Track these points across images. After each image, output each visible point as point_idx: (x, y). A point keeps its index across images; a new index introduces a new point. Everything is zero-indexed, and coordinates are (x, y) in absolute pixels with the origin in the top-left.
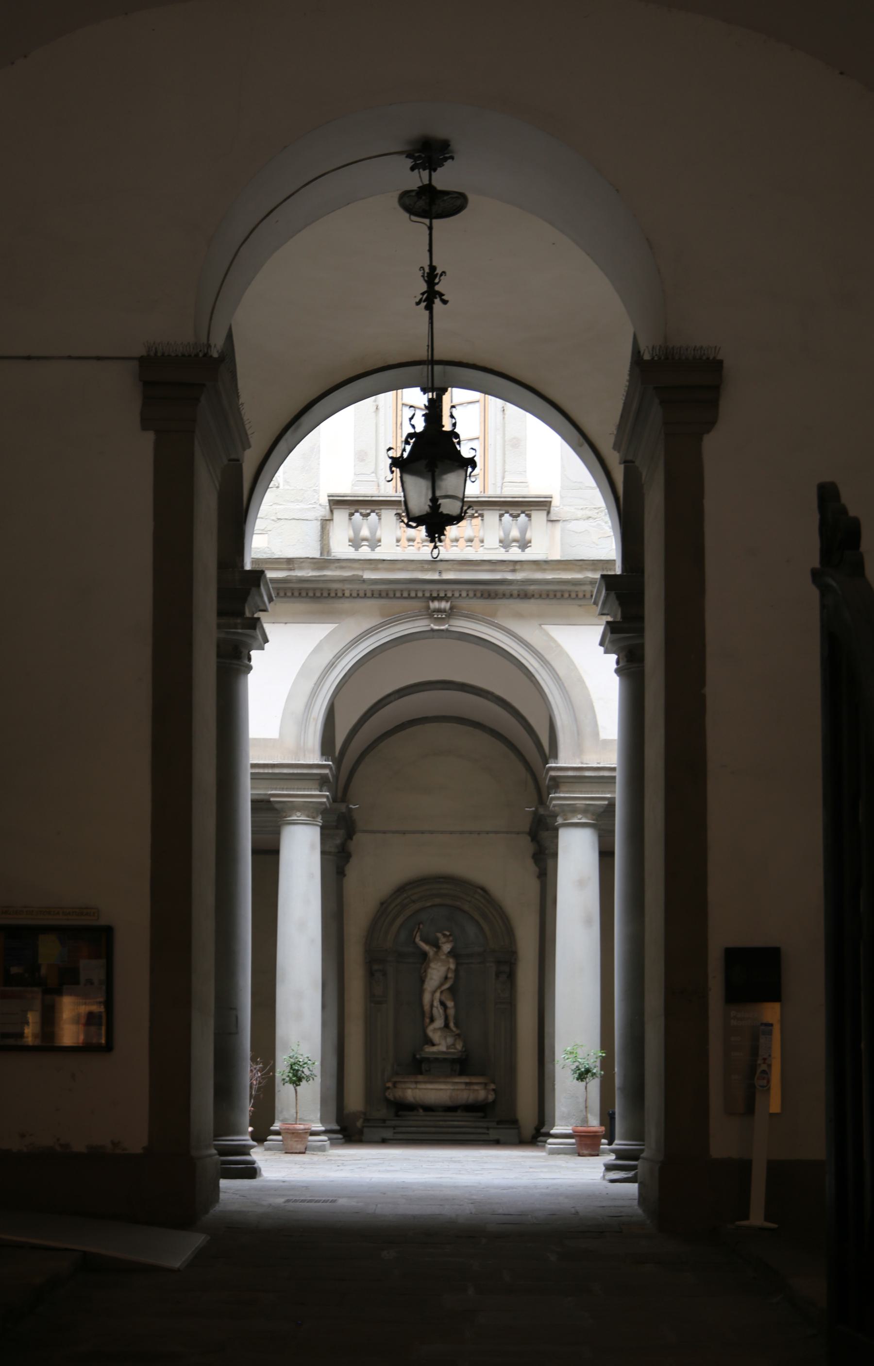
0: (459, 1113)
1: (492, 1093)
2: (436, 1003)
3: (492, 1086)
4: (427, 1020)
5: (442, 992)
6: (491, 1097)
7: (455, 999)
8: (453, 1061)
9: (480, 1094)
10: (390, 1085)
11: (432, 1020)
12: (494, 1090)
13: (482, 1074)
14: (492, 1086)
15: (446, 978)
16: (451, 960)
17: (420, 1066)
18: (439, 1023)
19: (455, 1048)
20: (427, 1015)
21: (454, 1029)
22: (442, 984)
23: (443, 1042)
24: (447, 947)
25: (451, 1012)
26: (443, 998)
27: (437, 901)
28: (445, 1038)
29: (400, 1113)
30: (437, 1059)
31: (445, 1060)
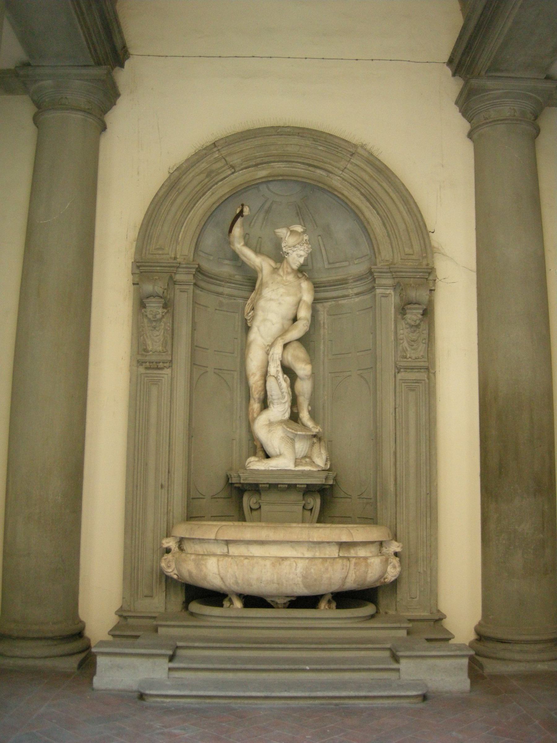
0: (325, 610)
1: (395, 561)
2: (274, 368)
3: (395, 547)
4: (256, 406)
5: (285, 346)
6: (392, 573)
7: (312, 358)
8: (309, 490)
9: (371, 568)
10: (170, 543)
11: (265, 404)
12: (396, 554)
13: (370, 520)
14: (395, 547)
15: (295, 319)
16: (305, 285)
17: (242, 497)
18: (279, 410)
19: (313, 463)
20: (256, 394)
21: (310, 424)
22: (284, 332)
23: (285, 449)
24: (297, 256)
25: (304, 387)
26: (289, 358)
27: (280, 168)
28: (292, 441)
29: (195, 607)
30: (273, 487)
31: (291, 487)
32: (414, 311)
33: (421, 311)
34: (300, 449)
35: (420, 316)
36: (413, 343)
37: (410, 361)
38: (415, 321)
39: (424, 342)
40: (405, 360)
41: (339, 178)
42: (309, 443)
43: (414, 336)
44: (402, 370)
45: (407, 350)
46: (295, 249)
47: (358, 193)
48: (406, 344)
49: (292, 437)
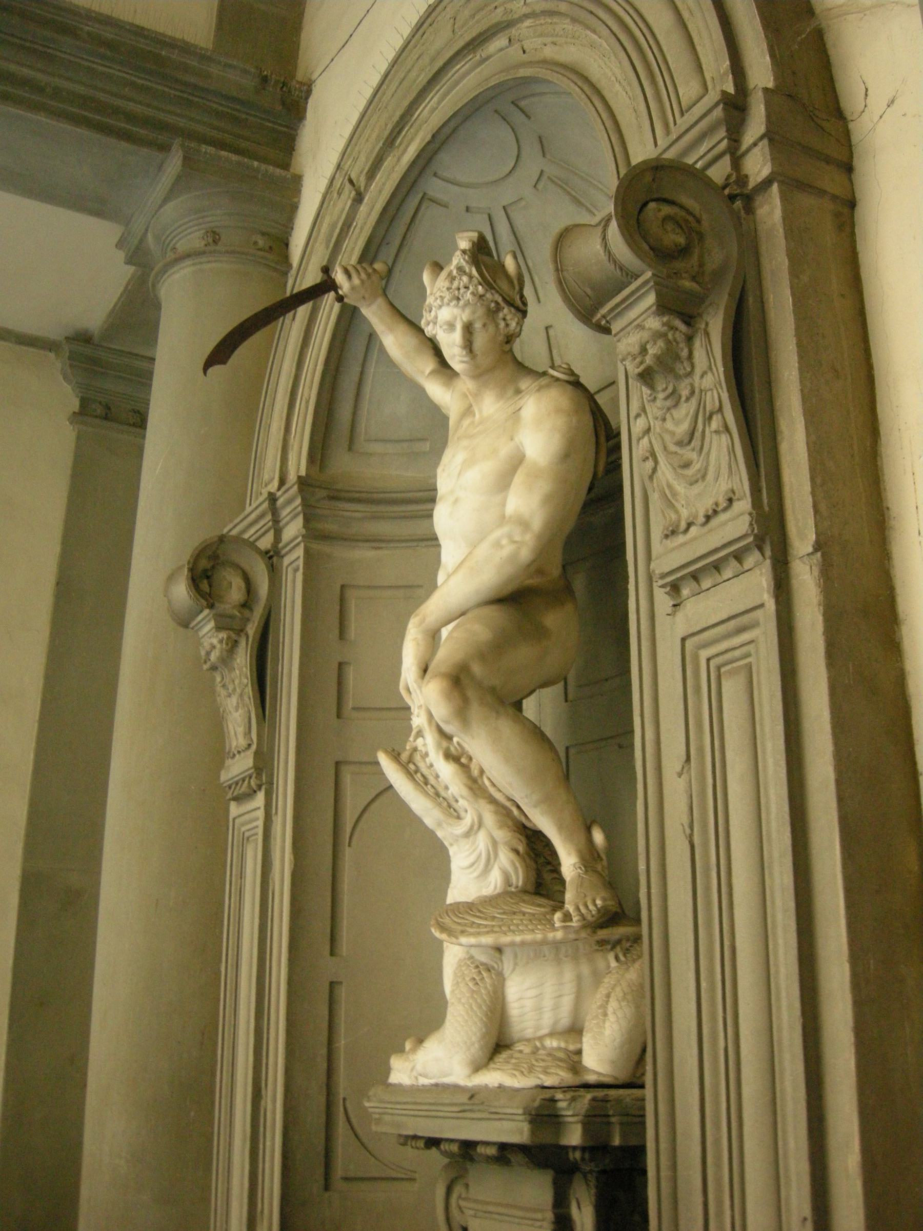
32: (633, 314)
33: (651, 299)
34: (529, 1004)
35: (654, 323)
36: (689, 453)
37: (694, 539)
38: (644, 350)
39: (715, 424)
40: (681, 539)
41: (528, 23)
42: (569, 974)
43: (680, 421)
44: (685, 592)
45: (674, 494)
46: (433, 313)
47: (566, 25)
48: (665, 472)
49: (482, 958)
